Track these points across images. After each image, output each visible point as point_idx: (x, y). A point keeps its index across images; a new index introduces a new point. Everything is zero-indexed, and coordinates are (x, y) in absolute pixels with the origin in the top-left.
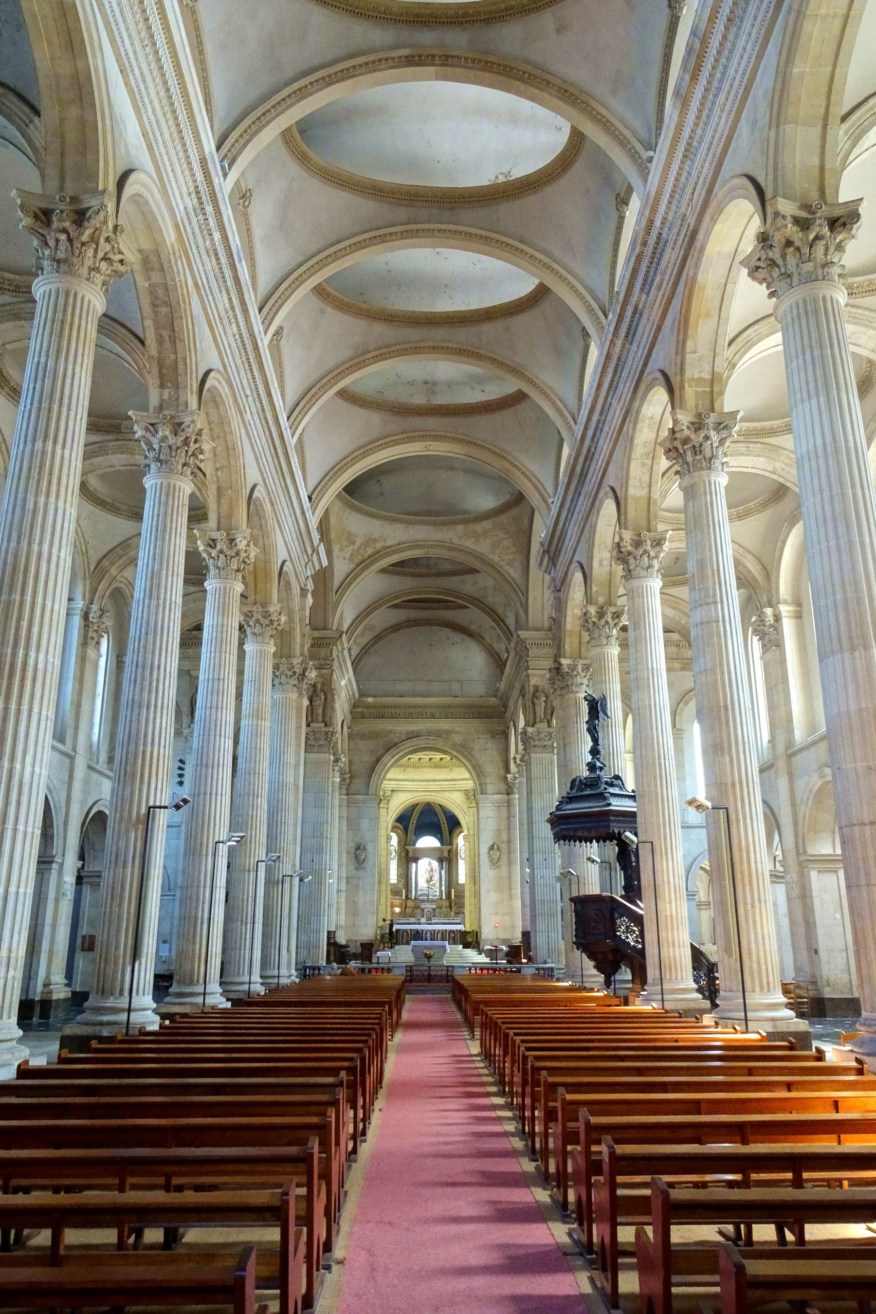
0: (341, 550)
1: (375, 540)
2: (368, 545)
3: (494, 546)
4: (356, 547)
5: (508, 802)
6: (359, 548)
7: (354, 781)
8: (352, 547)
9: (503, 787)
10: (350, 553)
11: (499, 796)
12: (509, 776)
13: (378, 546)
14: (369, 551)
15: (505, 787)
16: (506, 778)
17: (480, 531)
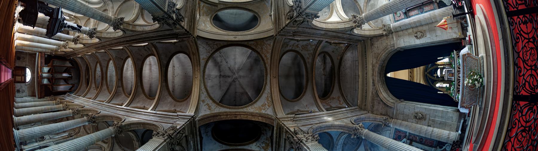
0: (264, 110)
1: (268, 96)
2: (268, 99)
3: (268, 52)
4: (267, 104)
5: (396, 32)
6: (268, 103)
7: (389, 114)
8: (266, 105)
9: (390, 36)
10: (267, 106)
11: (394, 37)
12: (384, 33)
13: (269, 96)
14: (270, 99)
15: (390, 34)
16: (386, 35)
17: (266, 58)
